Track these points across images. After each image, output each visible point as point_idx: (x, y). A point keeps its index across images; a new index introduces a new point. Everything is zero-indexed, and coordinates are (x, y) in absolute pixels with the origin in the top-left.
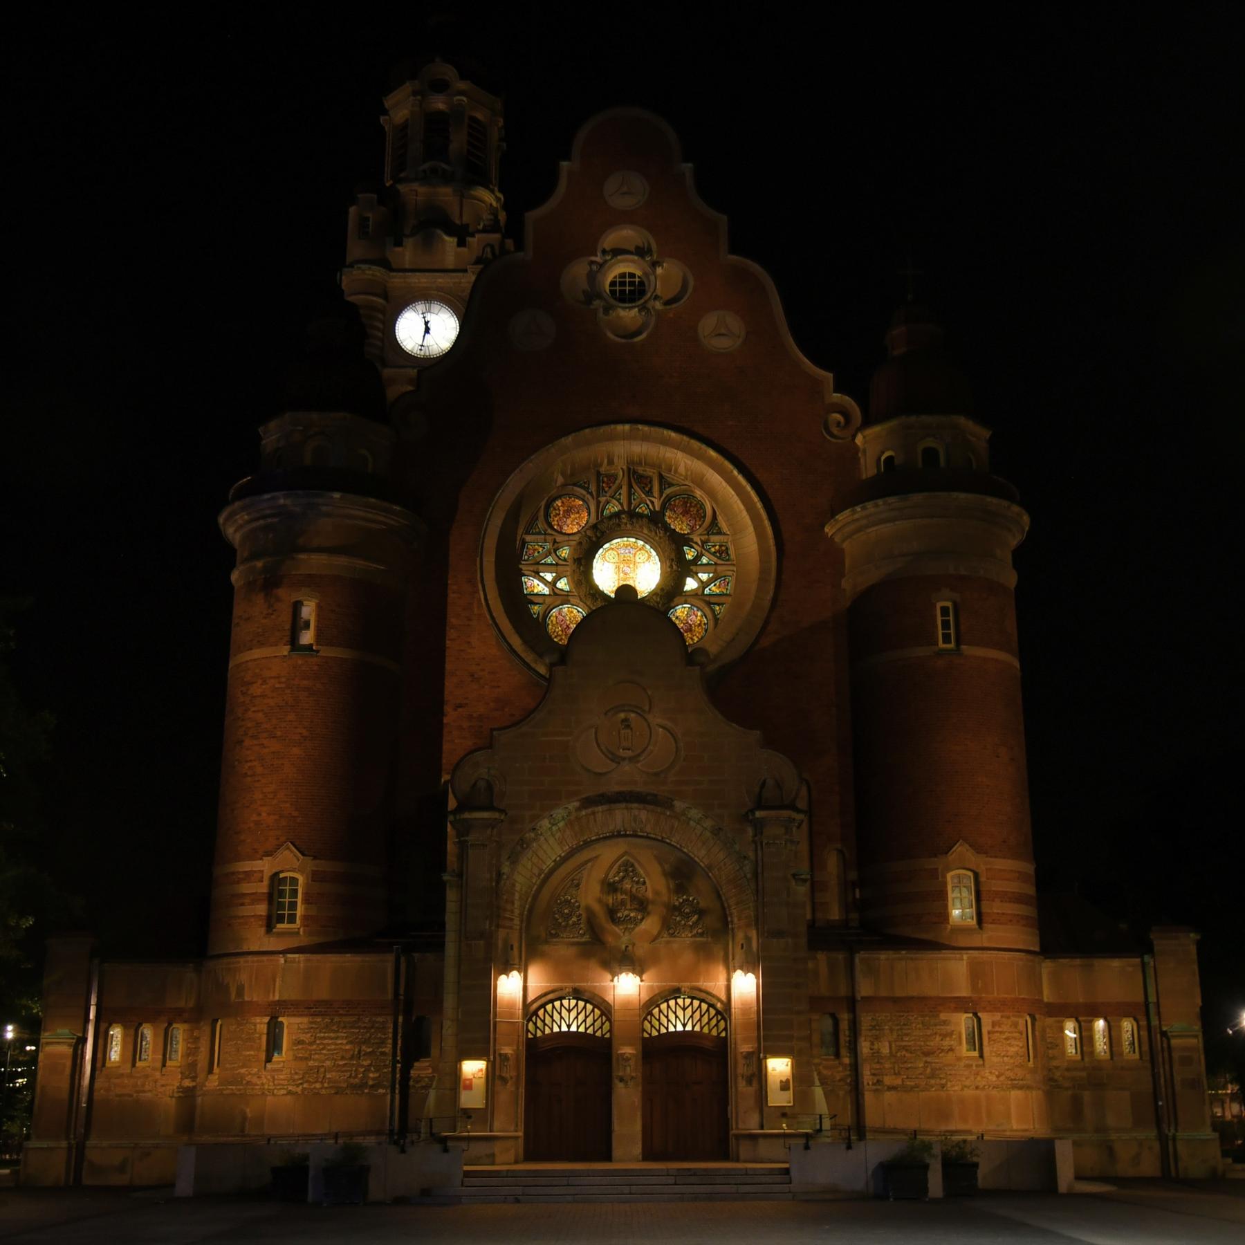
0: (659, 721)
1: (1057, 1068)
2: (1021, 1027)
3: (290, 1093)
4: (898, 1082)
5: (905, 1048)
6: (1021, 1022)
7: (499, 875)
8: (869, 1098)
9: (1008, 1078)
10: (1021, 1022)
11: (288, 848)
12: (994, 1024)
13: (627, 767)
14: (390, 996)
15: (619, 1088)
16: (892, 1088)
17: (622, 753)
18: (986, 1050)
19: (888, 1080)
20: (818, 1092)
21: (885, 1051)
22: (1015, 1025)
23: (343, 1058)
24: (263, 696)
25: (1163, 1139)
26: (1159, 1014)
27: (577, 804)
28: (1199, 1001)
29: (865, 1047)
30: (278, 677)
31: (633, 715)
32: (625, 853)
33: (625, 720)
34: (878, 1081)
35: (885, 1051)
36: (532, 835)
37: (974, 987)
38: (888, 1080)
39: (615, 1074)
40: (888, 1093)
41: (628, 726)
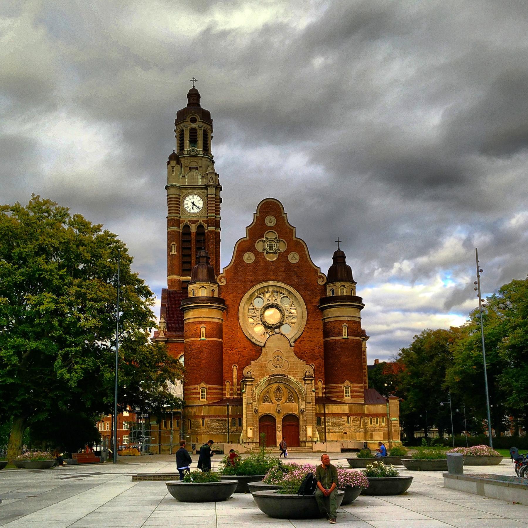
0: (284, 359)
1: (367, 428)
2: (359, 419)
3: (207, 434)
4: (333, 431)
5: (335, 424)
6: (359, 418)
7: (253, 391)
8: (327, 434)
9: (356, 430)
10: (359, 418)
11: (203, 383)
12: (353, 419)
13: (278, 368)
14: (227, 414)
15: (278, 432)
16: (332, 432)
17: (277, 366)
18: (352, 424)
19: (331, 430)
20: (317, 433)
21: (330, 424)
22: (358, 419)
23: (217, 427)
24: (195, 349)
25: (389, 442)
26: (389, 416)
27: (269, 376)
28: (399, 413)
29: (326, 423)
30: (198, 345)
31: (279, 358)
32: (278, 386)
33: (278, 359)
34: (329, 431)
35: (330, 424)
36: (260, 383)
37: (349, 412)
38: (331, 430)
39: (277, 430)
40: (331, 433)
41: (278, 360)
